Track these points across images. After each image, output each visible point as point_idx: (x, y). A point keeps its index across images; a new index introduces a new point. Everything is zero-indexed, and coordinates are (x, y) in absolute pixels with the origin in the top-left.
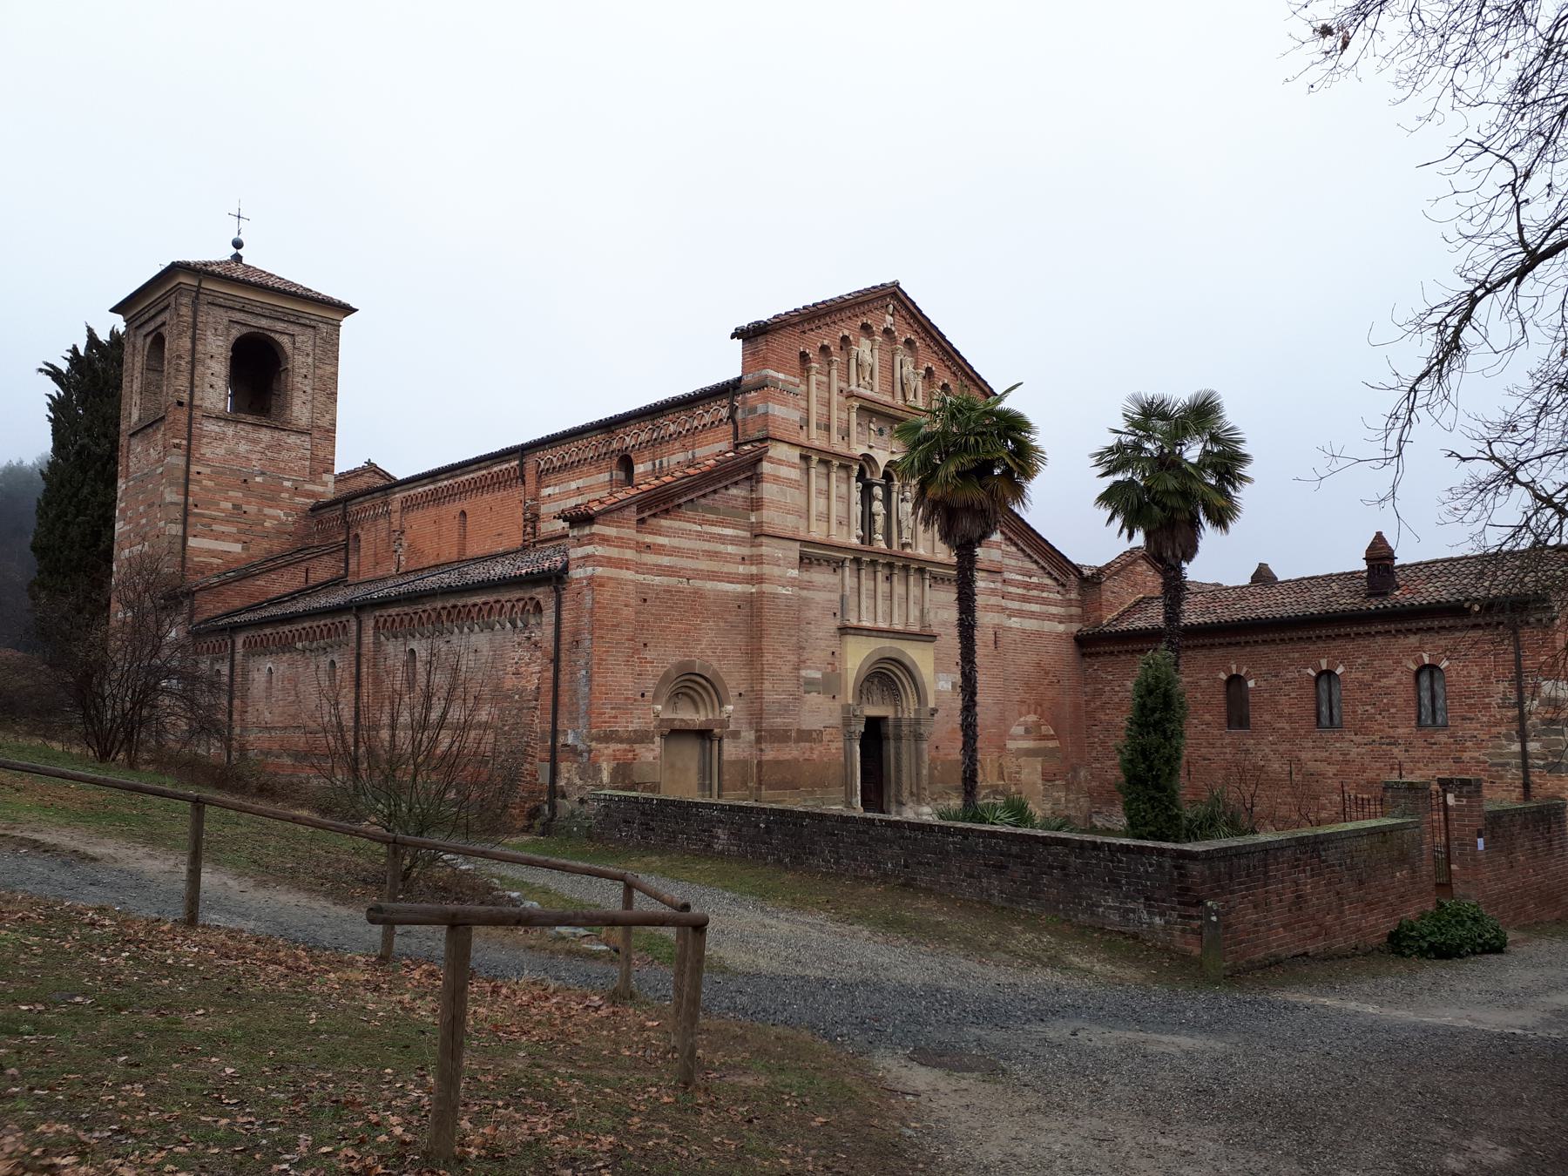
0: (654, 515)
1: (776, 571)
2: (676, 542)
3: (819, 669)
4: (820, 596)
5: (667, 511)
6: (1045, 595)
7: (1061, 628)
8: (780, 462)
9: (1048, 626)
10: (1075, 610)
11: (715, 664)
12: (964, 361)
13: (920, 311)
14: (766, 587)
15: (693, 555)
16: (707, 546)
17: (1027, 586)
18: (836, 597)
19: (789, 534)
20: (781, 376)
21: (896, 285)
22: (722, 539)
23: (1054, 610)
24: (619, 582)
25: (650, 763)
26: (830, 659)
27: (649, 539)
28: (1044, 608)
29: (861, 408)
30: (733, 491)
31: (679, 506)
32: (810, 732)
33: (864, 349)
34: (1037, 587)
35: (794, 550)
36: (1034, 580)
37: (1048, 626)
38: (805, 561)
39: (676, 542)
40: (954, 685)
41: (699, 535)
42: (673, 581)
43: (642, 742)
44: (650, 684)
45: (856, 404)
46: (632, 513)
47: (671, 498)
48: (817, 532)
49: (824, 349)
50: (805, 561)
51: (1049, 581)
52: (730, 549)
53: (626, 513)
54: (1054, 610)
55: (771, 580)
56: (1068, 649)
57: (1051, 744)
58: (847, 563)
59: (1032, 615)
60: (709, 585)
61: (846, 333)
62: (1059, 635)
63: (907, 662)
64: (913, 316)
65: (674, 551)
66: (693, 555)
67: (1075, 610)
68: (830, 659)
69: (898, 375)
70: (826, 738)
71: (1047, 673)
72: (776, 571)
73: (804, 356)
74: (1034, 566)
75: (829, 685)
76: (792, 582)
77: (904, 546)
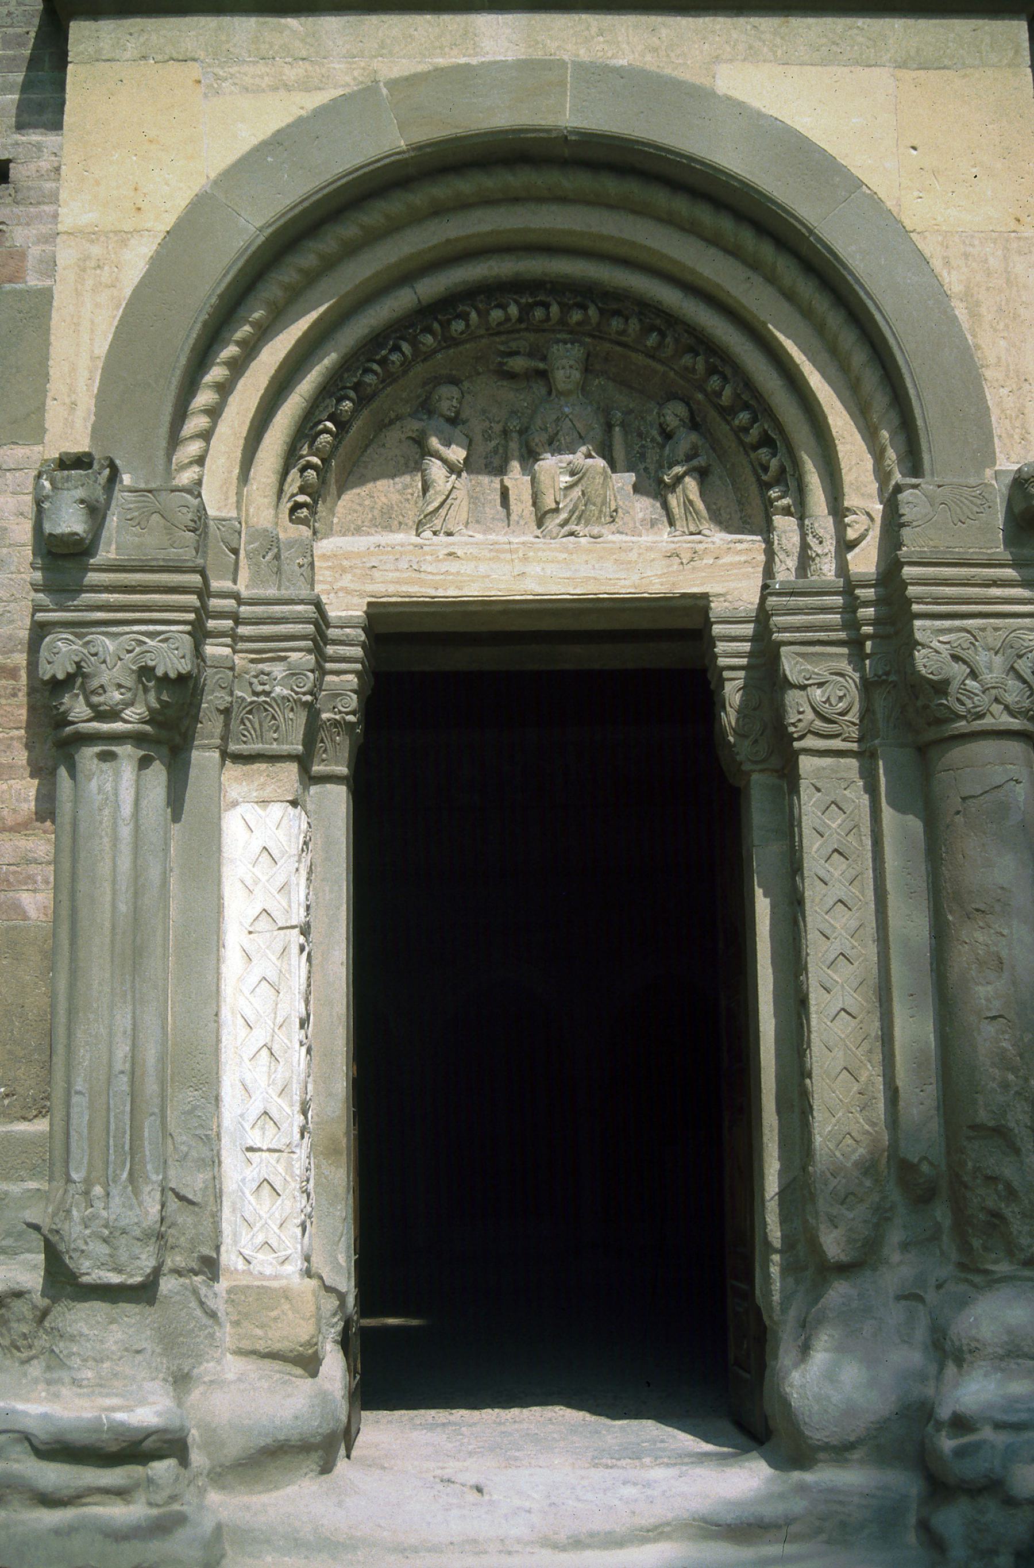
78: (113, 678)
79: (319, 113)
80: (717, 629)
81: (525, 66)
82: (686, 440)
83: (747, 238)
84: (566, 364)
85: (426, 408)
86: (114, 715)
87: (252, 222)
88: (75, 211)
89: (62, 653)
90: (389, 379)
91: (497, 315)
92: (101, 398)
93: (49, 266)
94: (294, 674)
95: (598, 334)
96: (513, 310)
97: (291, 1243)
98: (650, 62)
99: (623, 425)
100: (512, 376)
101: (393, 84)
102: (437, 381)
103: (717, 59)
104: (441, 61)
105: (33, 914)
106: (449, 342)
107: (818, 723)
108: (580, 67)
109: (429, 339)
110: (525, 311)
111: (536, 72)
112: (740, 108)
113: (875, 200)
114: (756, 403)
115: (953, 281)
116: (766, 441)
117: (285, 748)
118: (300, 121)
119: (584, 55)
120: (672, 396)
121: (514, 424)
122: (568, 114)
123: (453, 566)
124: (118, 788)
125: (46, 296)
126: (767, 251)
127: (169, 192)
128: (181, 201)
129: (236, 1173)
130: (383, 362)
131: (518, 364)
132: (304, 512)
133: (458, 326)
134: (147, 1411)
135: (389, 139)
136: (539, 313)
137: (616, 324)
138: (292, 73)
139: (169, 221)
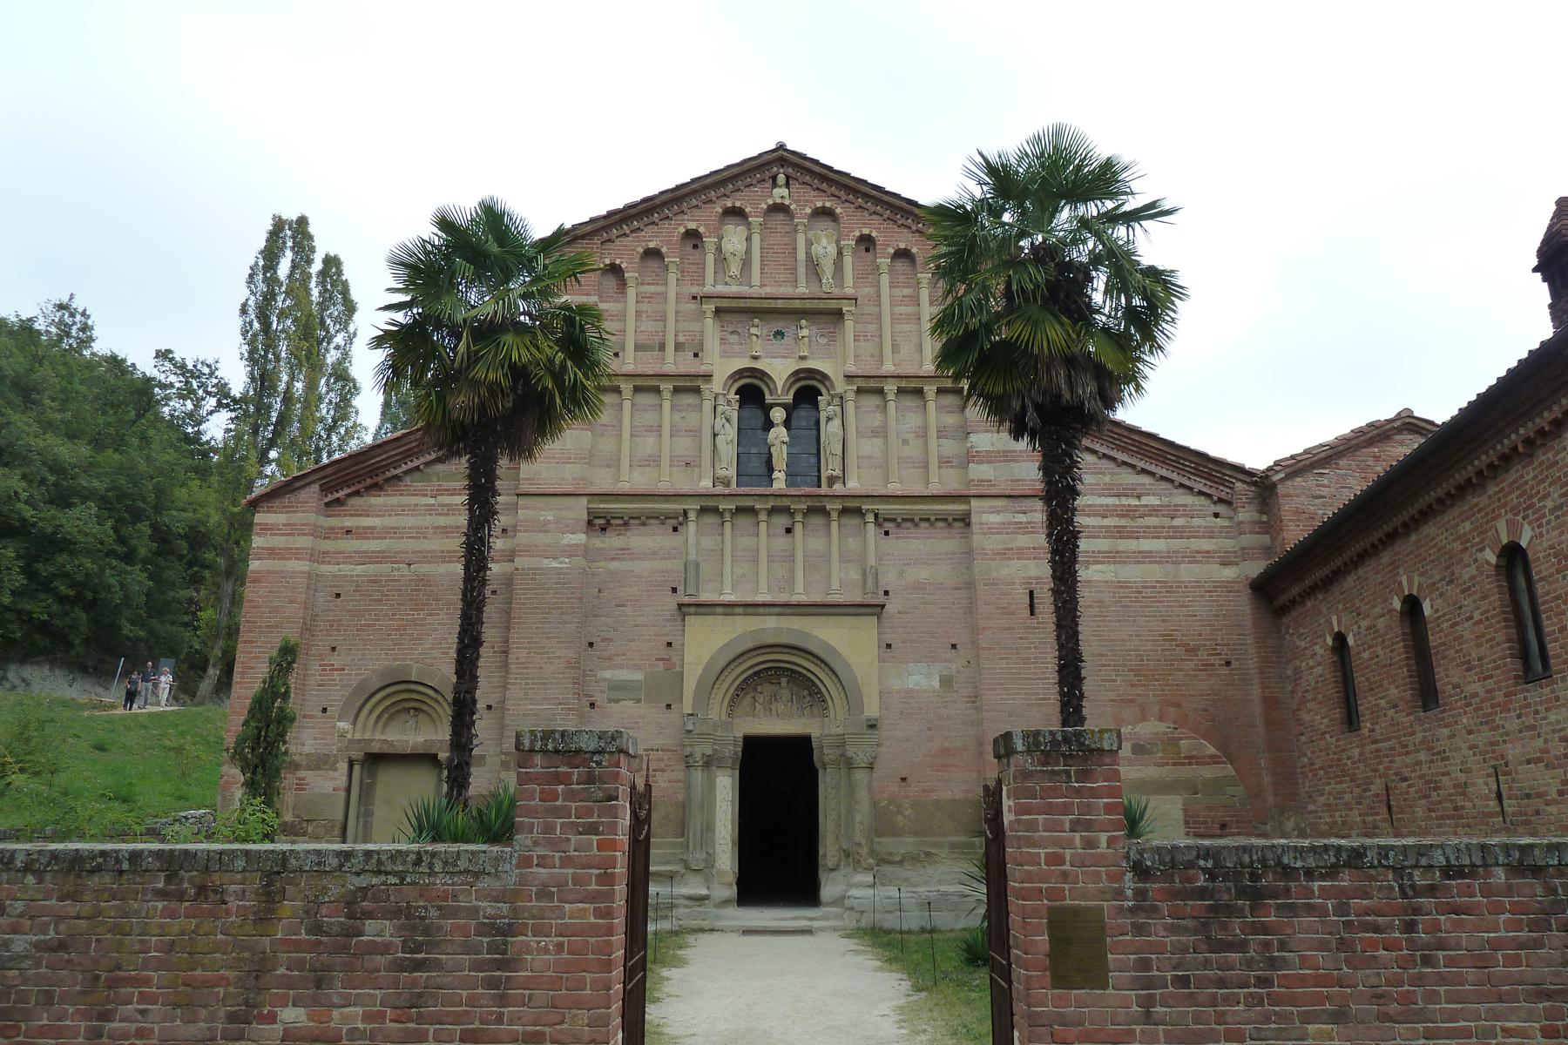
0: (357, 493)
1: (541, 539)
2: (391, 521)
3: (639, 668)
5: (377, 487)
6: (1178, 522)
7: (1229, 573)
9: (1188, 572)
10: (1248, 540)
13: (830, 168)
14: (520, 562)
15: (420, 534)
17: (1128, 512)
18: (677, 565)
19: (570, 489)
21: (781, 147)
23: (1205, 545)
24: (282, 574)
25: (328, 796)
27: (349, 522)
28: (1178, 544)
29: (718, 312)
31: (397, 478)
33: (734, 238)
34: (1153, 511)
35: (578, 510)
36: (1145, 500)
37: (1188, 572)
38: (599, 523)
39: (391, 521)
40: (946, 682)
41: (430, 510)
42: (385, 568)
43: (319, 768)
44: (336, 697)
45: (710, 307)
46: (312, 493)
47: (375, 471)
48: (603, 481)
49: (653, 254)
50: (599, 523)
51: (1189, 500)
53: (303, 495)
54: (1205, 545)
55: (529, 551)
56: (1244, 604)
57: (1208, 772)
58: (692, 516)
59: (1145, 557)
61: (692, 226)
62: (1226, 586)
64: (823, 178)
65: (386, 533)
66: (420, 534)
67: (1248, 540)
68: (663, 652)
69: (801, 255)
71: (1192, 651)
72: (541, 539)
73: (615, 270)
74: (1146, 479)
75: (664, 687)
76: (571, 551)
77: (832, 481)
78: (698, 756)
84: (784, 681)
85: (755, 690)
87: (723, 662)
89: (688, 750)
97: (728, 863)
111: (778, 630)
114: (820, 692)
122: (784, 640)
124: (698, 776)
127: (706, 656)
129: (719, 849)
134: (704, 892)
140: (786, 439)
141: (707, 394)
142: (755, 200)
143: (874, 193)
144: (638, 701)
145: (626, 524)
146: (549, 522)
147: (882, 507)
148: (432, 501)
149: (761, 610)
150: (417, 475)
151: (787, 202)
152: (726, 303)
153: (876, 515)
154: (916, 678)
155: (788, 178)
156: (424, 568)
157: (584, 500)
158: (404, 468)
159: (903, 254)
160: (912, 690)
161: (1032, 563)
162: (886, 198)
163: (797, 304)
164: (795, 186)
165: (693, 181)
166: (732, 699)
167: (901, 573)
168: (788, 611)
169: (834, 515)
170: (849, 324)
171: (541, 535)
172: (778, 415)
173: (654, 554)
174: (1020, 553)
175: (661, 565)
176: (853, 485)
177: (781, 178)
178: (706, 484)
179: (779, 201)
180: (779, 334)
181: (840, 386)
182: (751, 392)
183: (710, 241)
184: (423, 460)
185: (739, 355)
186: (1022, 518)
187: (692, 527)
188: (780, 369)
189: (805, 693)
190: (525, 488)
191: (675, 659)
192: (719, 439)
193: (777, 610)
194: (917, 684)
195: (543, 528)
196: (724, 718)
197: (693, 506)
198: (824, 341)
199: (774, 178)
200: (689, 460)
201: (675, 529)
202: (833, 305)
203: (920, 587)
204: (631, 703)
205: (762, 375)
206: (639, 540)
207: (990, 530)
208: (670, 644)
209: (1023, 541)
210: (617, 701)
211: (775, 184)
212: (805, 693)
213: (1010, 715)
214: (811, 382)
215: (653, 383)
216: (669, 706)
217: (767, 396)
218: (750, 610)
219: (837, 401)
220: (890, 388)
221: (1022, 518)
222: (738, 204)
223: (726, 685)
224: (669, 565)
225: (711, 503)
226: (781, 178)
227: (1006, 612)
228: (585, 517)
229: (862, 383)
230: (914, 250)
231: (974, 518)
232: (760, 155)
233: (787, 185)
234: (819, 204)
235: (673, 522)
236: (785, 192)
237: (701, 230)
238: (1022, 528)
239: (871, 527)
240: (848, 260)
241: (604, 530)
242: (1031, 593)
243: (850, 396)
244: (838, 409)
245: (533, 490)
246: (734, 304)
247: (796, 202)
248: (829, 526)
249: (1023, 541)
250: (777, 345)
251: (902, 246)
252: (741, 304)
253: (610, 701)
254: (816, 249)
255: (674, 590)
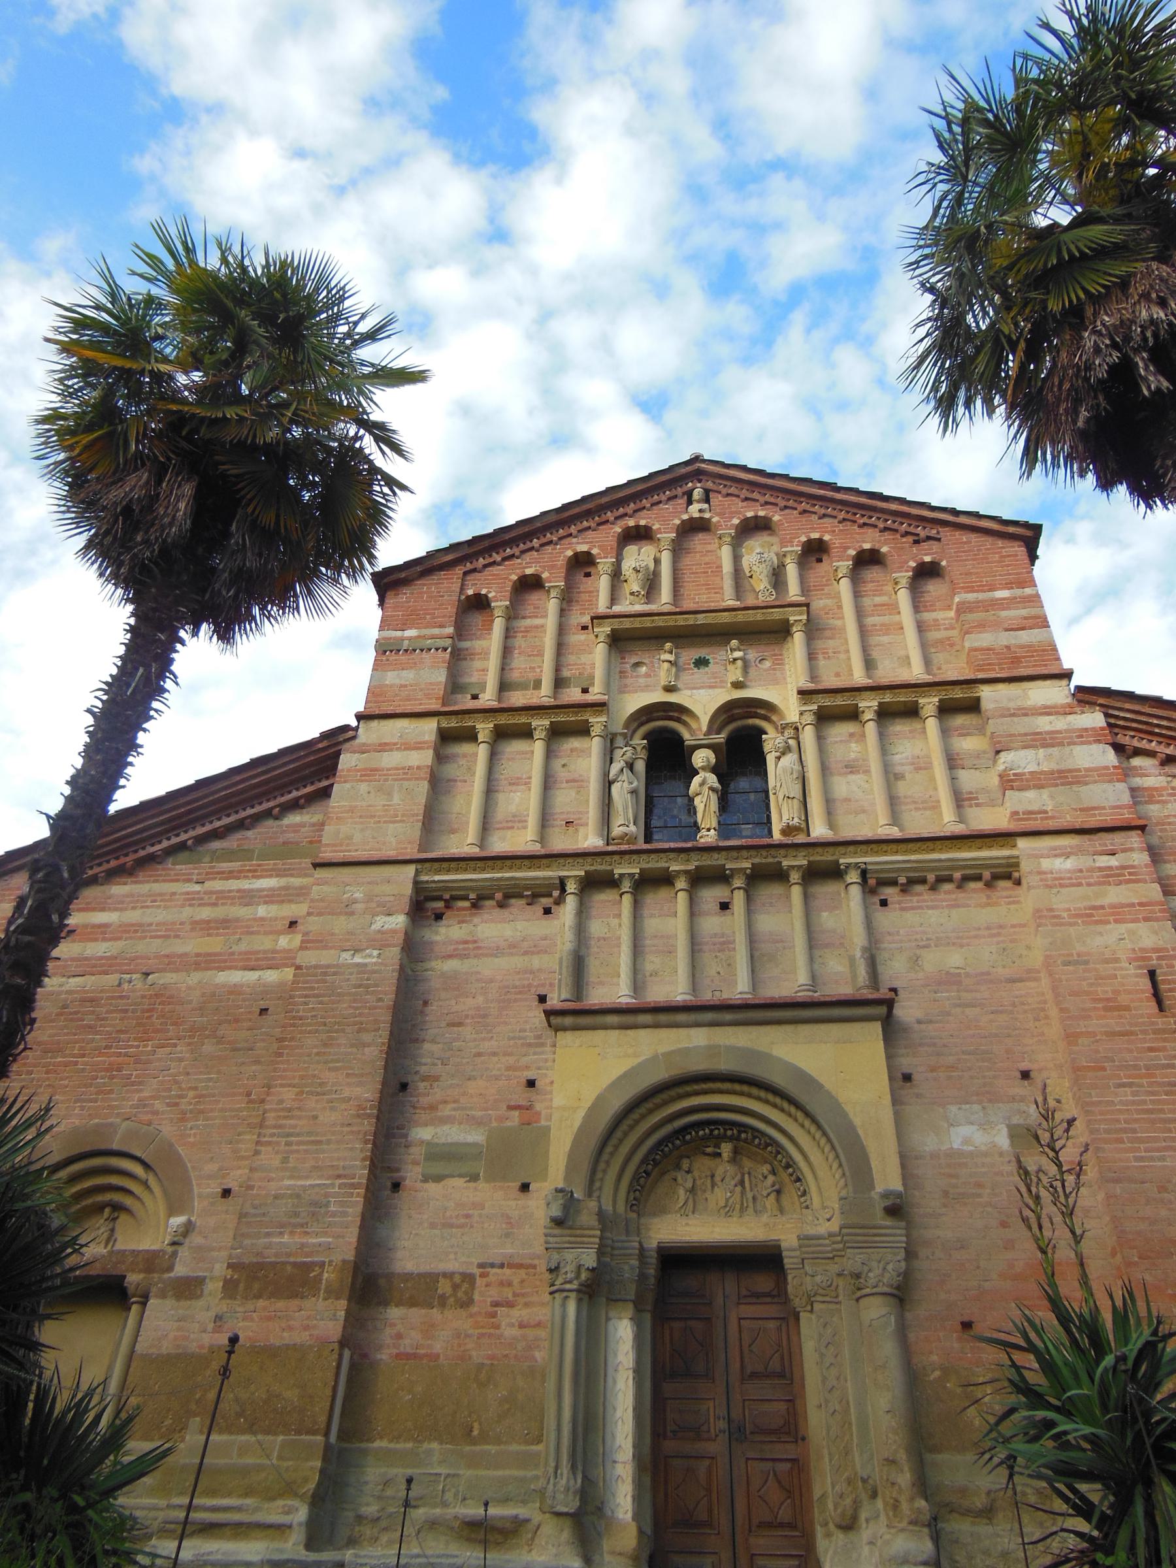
1: (340, 924)
3: (478, 1123)
4: (488, 967)
8: (383, 747)
11: (168, 1130)
12: (902, 501)
15: (170, 932)
16: (205, 913)
20: (411, 633)
21: (697, 459)
22: (248, 898)
26: (521, 1096)
30: (294, 818)
32: (431, 1279)
39: (133, 916)
41: (191, 900)
45: (605, 629)
52: (262, 911)
58: (571, 887)
60: (195, 978)
61: (583, 548)
63: (778, 1080)
68: (521, 1096)
70: (483, 1295)
79: (639, 1064)
80: (784, 1254)
81: (709, 1047)
82: (771, 1179)
83: (786, 1105)
84: (726, 1149)
85: (678, 1167)
86: (570, 1282)
87: (617, 1103)
88: (558, 1100)
90: (665, 1156)
91: (701, 1133)
92: (567, 1167)
93: (549, 1118)
94: (632, 1268)
95: (738, 1139)
96: (707, 1131)
98: (749, 1045)
99: (749, 1173)
100: (708, 1155)
101: (663, 1054)
102: (681, 1157)
103: (773, 1043)
104: (680, 1046)
105: (539, 1359)
106: (685, 1143)
107: (820, 1291)
108: (726, 1047)
109: (678, 1142)
110: (711, 1131)
111: (712, 1051)
112: (780, 1060)
113: (828, 1092)
115: (857, 1121)
116: (798, 1180)
117: (628, 1297)
118: (633, 1068)
119: (728, 1043)
120: (766, 1162)
121: (709, 1173)
122: (724, 1065)
123: (687, 1228)
125: (548, 1128)
126: (793, 1110)
128: (594, 1096)
130: (662, 1151)
131: (709, 1150)
132: (635, 1208)
133: (688, 1137)
135: (661, 1074)
136: (716, 1132)
137: (743, 1136)
138: (630, 1051)
139: (589, 1104)
140: (717, 785)
141: (596, 730)
142: (665, 519)
143: (822, 492)
144: (474, 1178)
145: (475, 906)
146: (355, 902)
147: (869, 859)
148: (197, 888)
149: (682, 1017)
150: (184, 855)
151: (707, 515)
152: (627, 624)
153: (864, 874)
154: (965, 1131)
155: (707, 492)
156: (169, 978)
157: (411, 870)
158: (165, 844)
159: (868, 560)
160: (960, 1153)
161: (1143, 929)
162: (839, 496)
163: (725, 618)
164: (716, 499)
165: (585, 499)
166: (636, 1178)
167: (915, 961)
168: (728, 1017)
169: (795, 877)
170: (798, 638)
171: (343, 918)
172: (702, 758)
173: (513, 947)
174: (1119, 913)
175: (518, 962)
176: (819, 830)
177: (697, 493)
178: (591, 840)
179: (696, 515)
180: (701, 663)
181: (791, 709)
182: (666, 755)
183: (605, 564)
184: (192, 833)
185: (647, 688)
186: (1113, 862)
187: (571, 902)
188: (703, 699)
189: (765, 1169)
190: (327, 855)
191: (538, 1107)
192: (615, 789)
193: (709, 1016)
194: (966, 1141)
195: (347, 908)
196: (621, 1207)
197: (574, 872)
198: (767, 664)
199: (689, 494)
200: (571, 818)
201: (547, 911)
202: (776, 614)
203: (950, 979)
204: (459, 1182)
205: (678, 712)
206: (492, 927)
207: (1059, 882)
208: (531, 1084)
209: (1115, 895)
210: (438, 1179)
211: (690, 502)
212: (765, 1169)
213: (1162, 1189)
214: (751, 721)
215: (523, 719)
216: (525, 1187)
217: (686, 735)
218: (663, 1018)
219: (789, 732)
220: (868, 705)
221: (1113, 862)
222: (643, 523)
223: (625, 1149)
224: (536, 962)
225: (599, 866)
226: (697, 493)
227: (1112, 1006)
228: (408, 890)
229: (827, 701)
230: (884, 549)
231: (1025, 866)
232: (672, 468)
233: (707, 501)
234: (750, 514)
235: (546, 901)
236: (706, 506)
237: (595, 551)
238: (1111, 876)
239: (855, 892)
240: (792, 571)
241: (439, 917)
242: (1152, 974)
243: (809, 718)
244: (792, 742)
245: (339, 856)
246: (637, 623)
247: (718, 514)
248: (788, 897)
249: (1115, 895)
250: (700, 674)
251: (867, 546)
252: (647, 623)
253: (426, 1179)
254: (745, 562)
255: (542, 999)
